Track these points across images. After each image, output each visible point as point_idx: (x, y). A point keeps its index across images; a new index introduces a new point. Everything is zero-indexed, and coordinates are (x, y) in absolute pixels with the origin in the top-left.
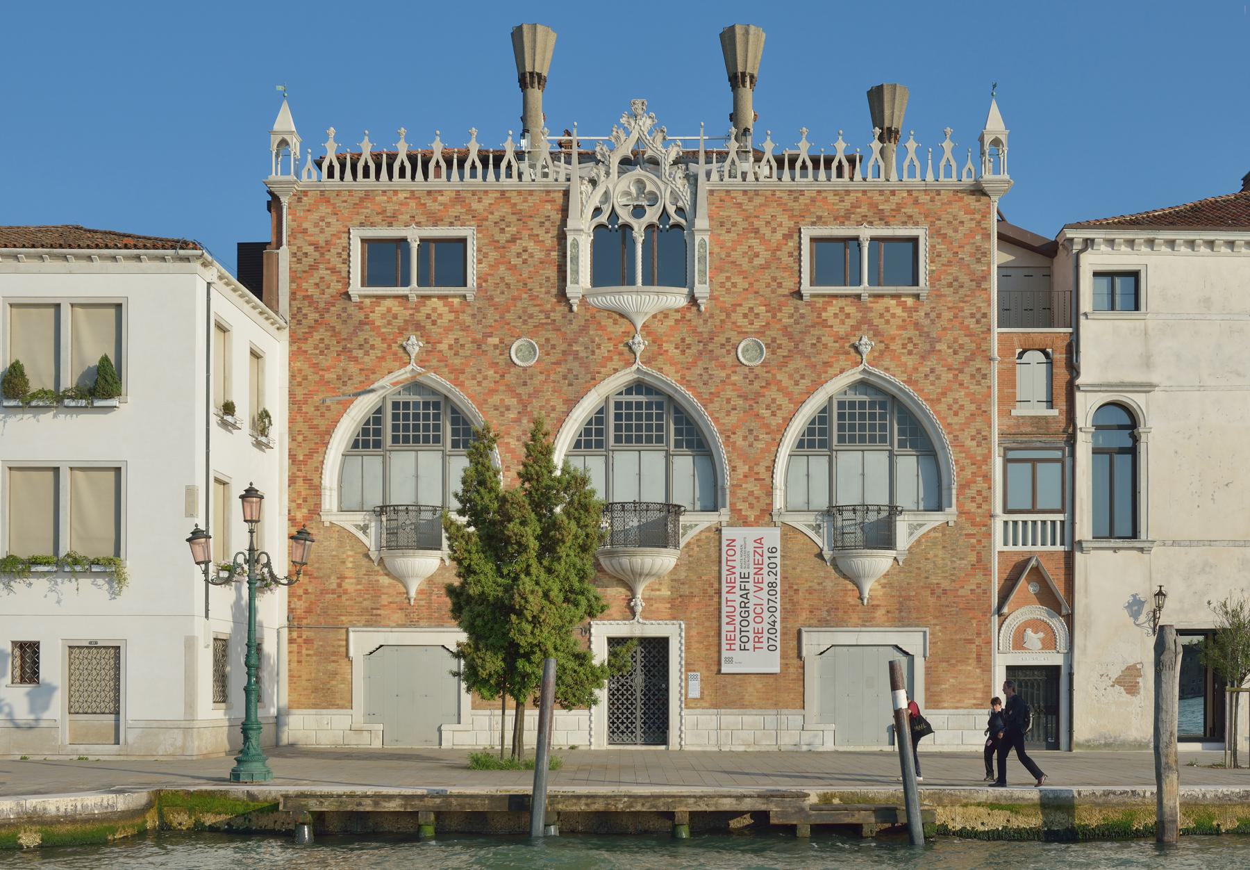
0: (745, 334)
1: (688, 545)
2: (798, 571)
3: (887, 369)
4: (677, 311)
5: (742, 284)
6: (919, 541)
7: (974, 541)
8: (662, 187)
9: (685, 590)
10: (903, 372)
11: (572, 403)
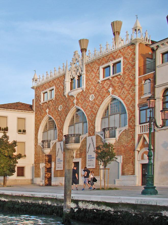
0: (91, 94)
3: (115, 94)
4: (81, 92)
5: (90, 83)
6: (121, 135)
7: (131, 133)
11: (66, 116)
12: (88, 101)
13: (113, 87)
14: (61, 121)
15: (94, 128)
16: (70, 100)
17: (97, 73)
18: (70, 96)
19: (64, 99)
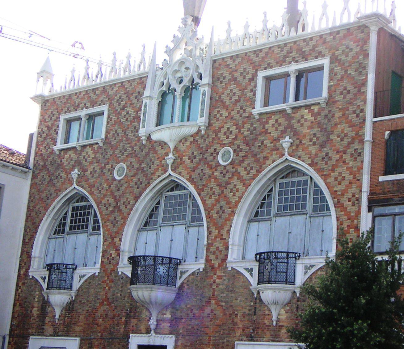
0: (223, 145)
1: (182, 284)
2: (238, 301)
3: (299, 158)
4: (192, 136)
5: (225, 113)
6: (310, 278)
9: (178, 314)
10: (309, 158)
11: (137, 198)
12: (214, 164)
13: (294, 135)
14: (120, 210)
15: (227, 249)
16: (156, 152)
17: (250, 88)
18: (156, 142)
19: (136, 148)
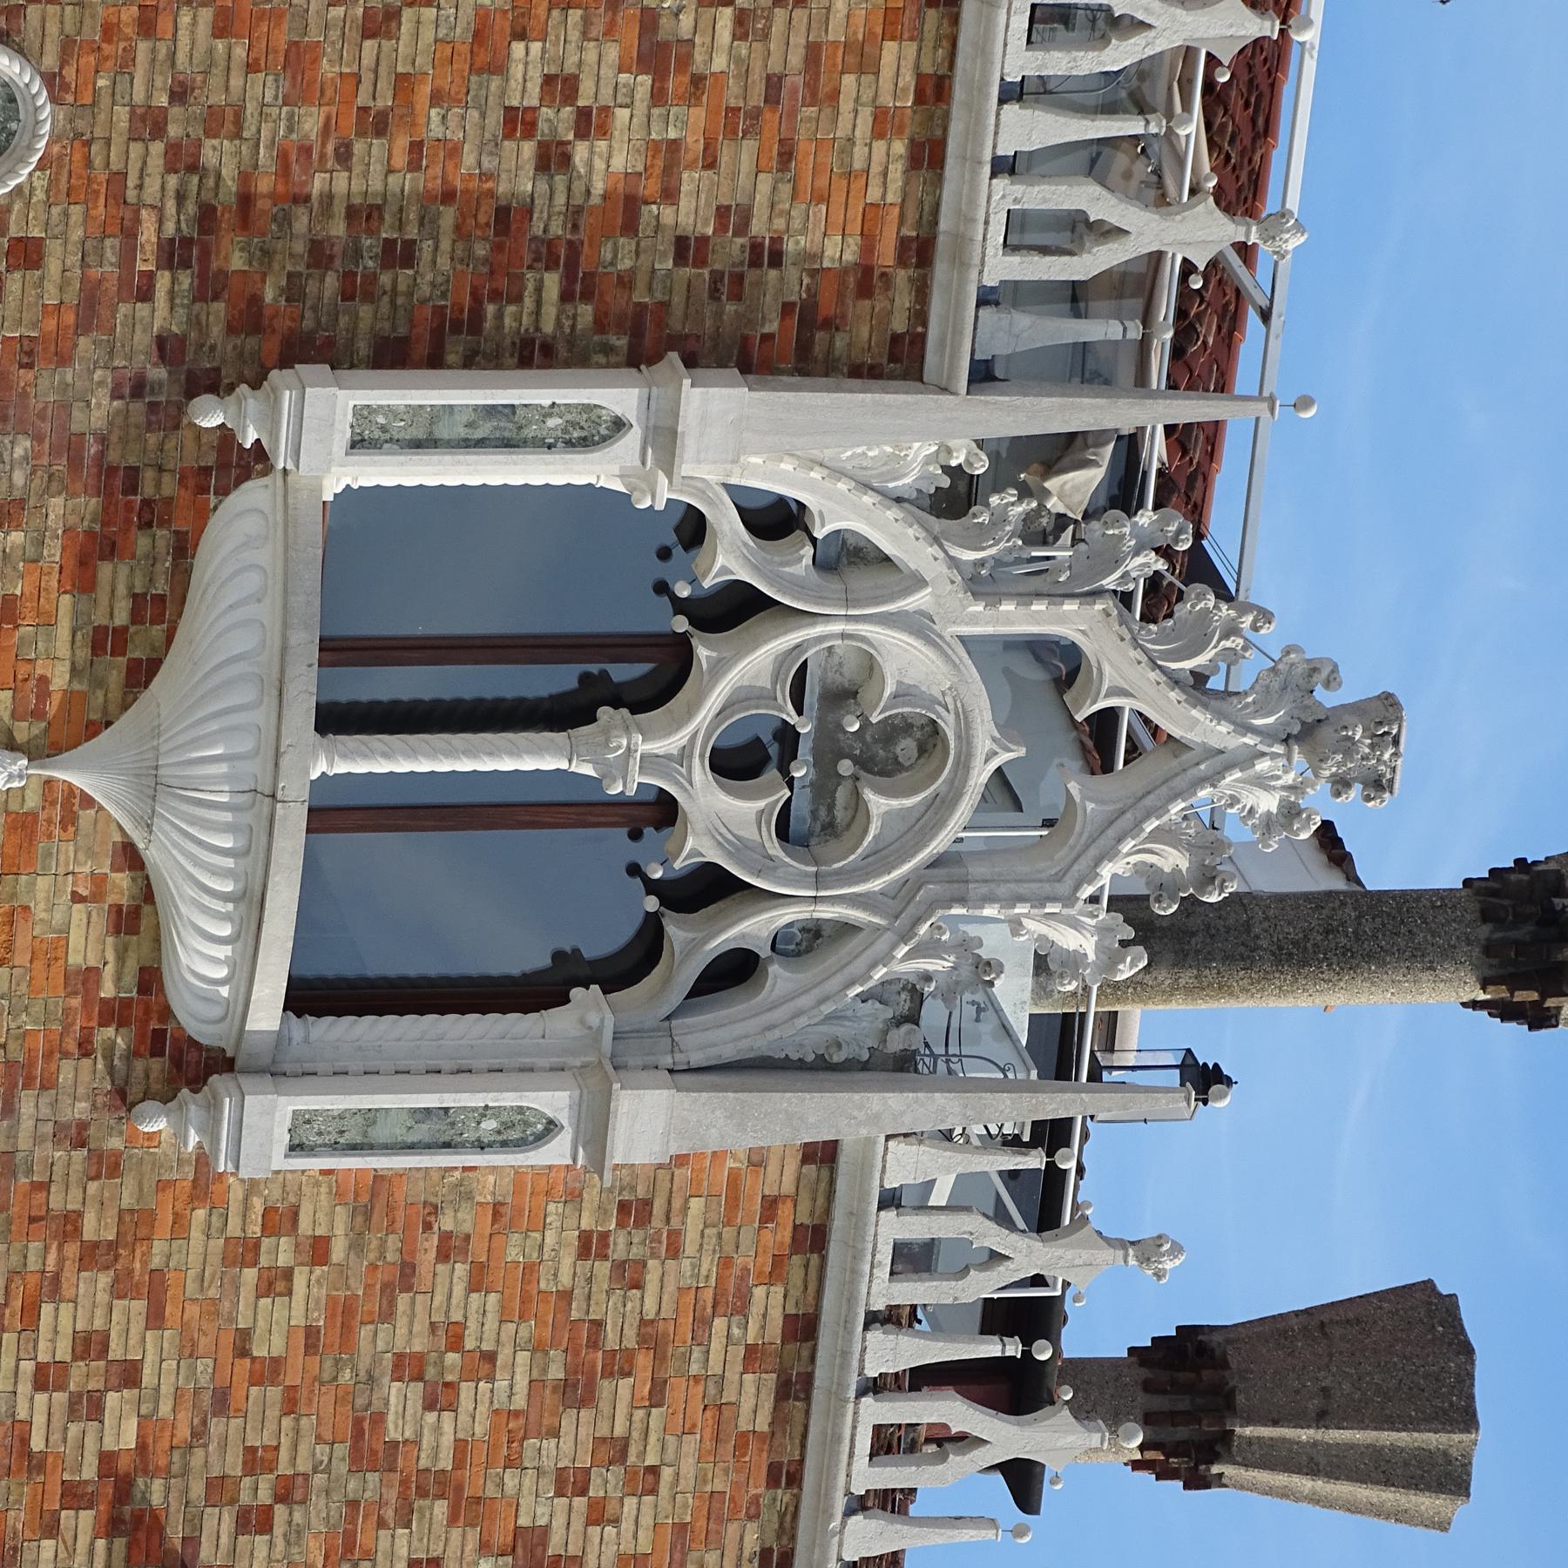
4: (150, 979)
8: (875, 885)
